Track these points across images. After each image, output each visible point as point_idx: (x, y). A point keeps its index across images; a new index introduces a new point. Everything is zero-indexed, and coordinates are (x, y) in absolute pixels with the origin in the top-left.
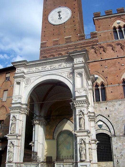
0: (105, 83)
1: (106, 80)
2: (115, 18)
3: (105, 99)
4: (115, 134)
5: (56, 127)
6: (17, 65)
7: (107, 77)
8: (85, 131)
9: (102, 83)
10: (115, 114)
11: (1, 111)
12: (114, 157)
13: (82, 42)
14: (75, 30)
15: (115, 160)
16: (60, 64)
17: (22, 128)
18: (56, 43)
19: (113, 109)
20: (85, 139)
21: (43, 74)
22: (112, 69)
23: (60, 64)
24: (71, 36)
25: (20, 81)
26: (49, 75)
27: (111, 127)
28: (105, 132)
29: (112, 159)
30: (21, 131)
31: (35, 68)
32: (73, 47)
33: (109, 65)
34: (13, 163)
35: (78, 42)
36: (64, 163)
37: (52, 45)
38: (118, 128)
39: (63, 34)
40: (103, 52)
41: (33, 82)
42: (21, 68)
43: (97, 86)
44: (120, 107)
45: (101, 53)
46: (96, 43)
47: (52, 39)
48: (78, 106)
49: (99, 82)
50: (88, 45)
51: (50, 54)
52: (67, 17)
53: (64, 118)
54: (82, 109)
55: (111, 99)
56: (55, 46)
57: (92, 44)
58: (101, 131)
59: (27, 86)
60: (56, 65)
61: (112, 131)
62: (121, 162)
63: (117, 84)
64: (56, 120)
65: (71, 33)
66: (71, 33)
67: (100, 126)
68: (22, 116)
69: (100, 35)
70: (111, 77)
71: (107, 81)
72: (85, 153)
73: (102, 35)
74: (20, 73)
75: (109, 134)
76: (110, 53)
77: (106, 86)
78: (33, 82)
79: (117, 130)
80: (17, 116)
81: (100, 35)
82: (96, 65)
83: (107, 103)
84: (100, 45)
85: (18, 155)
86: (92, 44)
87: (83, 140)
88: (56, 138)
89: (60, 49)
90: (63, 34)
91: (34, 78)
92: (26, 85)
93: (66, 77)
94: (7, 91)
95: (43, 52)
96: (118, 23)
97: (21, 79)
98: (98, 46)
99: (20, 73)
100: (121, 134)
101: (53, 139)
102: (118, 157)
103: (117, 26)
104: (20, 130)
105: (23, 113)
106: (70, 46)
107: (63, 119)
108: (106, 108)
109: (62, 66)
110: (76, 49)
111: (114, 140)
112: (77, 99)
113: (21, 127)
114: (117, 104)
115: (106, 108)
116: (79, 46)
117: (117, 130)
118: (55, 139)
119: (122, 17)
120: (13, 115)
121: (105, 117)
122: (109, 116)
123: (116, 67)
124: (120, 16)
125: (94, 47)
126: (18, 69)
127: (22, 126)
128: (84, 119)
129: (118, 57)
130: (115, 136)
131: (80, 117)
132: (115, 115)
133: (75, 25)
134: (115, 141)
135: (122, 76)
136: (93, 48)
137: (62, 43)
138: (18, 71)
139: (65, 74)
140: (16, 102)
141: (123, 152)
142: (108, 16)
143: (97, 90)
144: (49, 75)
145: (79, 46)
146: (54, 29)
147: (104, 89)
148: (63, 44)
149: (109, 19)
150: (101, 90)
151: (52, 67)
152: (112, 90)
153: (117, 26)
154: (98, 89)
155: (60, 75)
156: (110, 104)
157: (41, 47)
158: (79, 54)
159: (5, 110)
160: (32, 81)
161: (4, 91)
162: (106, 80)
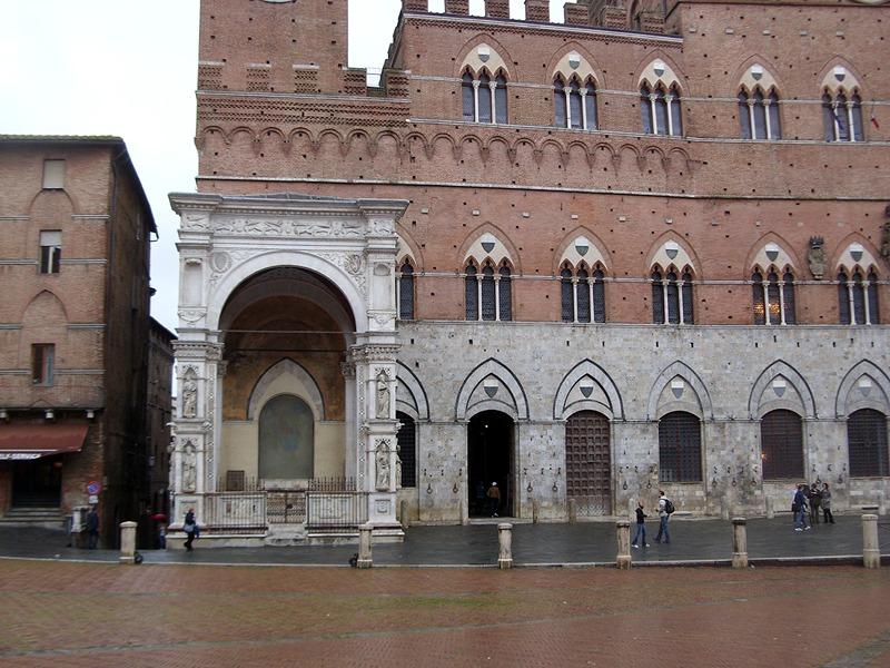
0: (416, 261)
2: (477, 33)
6: (186, 204)
7: (423, 246)
11: (38, 308)
13: (356, 104)
14: (334, 42)
15: (423, 485)
18: (259, 79)
19: (433, 347)
21: (270, 245)
22: (443, 220)
23: (324, 223)
24: (317, 67)
25: (199, 261)
26: (290, 251)
27: (419, 396)
31: (243, 221)
32: (324, 114)
35: (344, 99)
37: (245, 86)
38: (440, 401)
39: (289, 51)
40: (421, 157)
44: (451, 343)
46: (400, 119)
47: (247, 61)
48: (376, 356)
50: (374, 117)
51: (237, 124)
56: (255, 94)
57: (387, 118)
59: (219, 275)
60: (314, 226)
61: (422, 407)
63: (451, 270)
65: (317, 55)
66: (317, 55)
69: (419, 91)
70: (436, 246)
73: (424, 89)
74: (199, 234)
75: (413, 414)
76: (440, 168)
77: (417, 273)
78: (239, 266)
81: (419, 91)
84: (414, 130)
86: (387, 118)
88: (256, 418)
89: (274, 112)
90: (289, 51)
91: (242, 252)
92: (216, 274)
93: (343, 269)
94: (58, 234)
95: (211, 110)
96: (484, 58)
97: (203, 254)
98: (407, 130)
99: (199, 234)
100: (446, 419)
101: (248, 419)
103: (477, 67)
105: (212, 360)
106: (311, 107)
108: (412, 341)
109: (330, 233)
110: (331, 126)
112: (373, 340)
114: (444, 332)
115: (412, 341)
116: (345, 115)
119: (497, 35)
121: (405, 366)
122: (417, 364)
123: (455, 216)
124: (493, 29)
125: (393, 129)
129: (464, 184)
133: (334, 23)
135: (468, 248)
136: (391, 134)
137: (281, 88)
138: (191, 223)
139: (337, 259)
141: (445, 464)
142: (453, 19)
144: (290, 251)
145: (349, 116)
146: (252, 15)
148: (284, 90)
149: (453, 32)
151: (300, 229)
153: (477, 67)
156: (424, 329)
157: (201, 85)
159: (55, 306)
160: (236, 263)
161: (42, 231)
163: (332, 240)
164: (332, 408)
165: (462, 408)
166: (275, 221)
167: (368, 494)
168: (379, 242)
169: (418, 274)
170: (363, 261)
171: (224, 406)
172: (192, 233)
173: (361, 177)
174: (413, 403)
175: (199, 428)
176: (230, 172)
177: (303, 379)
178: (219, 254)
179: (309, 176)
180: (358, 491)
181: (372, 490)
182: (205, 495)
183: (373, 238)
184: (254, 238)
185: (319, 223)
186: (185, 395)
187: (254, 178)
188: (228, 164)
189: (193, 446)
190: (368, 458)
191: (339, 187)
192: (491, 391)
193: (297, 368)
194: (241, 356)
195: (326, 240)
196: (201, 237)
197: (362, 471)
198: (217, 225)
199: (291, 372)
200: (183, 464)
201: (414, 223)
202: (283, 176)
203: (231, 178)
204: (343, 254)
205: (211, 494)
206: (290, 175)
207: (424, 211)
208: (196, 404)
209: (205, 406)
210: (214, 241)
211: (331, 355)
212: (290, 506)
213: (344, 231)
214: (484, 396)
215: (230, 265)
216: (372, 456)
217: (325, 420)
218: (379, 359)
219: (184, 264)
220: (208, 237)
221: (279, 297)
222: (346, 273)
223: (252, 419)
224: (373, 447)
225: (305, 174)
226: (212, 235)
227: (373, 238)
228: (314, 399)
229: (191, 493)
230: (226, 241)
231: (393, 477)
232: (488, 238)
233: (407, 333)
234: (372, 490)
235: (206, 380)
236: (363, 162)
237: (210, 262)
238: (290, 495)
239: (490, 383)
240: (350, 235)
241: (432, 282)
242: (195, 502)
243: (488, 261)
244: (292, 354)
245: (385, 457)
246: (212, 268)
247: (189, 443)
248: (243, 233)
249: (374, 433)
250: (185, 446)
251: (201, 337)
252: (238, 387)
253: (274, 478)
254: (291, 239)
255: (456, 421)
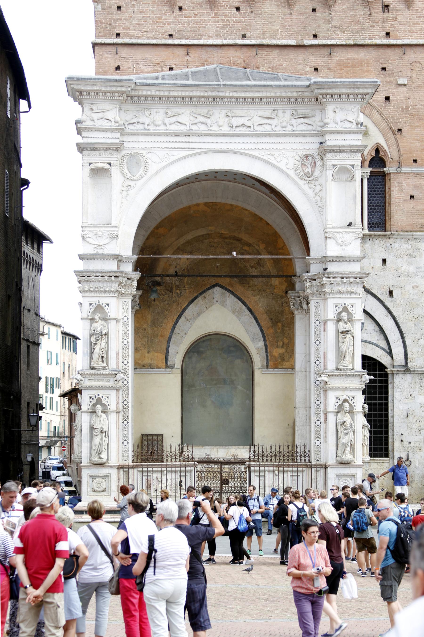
1: (397, 141)
4: (406, 363)
5: (180, 317)
7: (400, 130)
8: (352, 376)
9: (377, 151)
10: (414, 287)
12: (397, 444)
16: (268, 114)
17: (125, 347)
19: (412, 269)
20: (354, 398)
23: (267, 112)
29: (387, 449)
30: (121, 360)
33: (414, 75)
34: (111, 467)
36: (297, 466)
41: (158, 172)
42: (107, 107)
45: (387, 6)
48: (336, 288)
53: (214, 286)
54: (348, 302)
55: (408, 228)
59: (132, 183)
62: (418, 462)
64: (178, 291)
68: (121, 304)
71: (397, 144)
72: (353, 441)
74: (106, 130)
75: (384, 359)
78: (158, 172)
79: (415, 350)
80: (108, 305)
82: (361, 63)
83: (391, 241)
85: (118, 440)
87: (348, 402)
88: (178, 365)
92: (128, 182)
97: (114, 158)
99: (106, 130)
102: (410, 443)
104: (118, 354)
107: (209, 289)
108: (384, 261)
112: (332, 268)
113: (121, 345)
115: (384, 261)
117: (415, 350)
118: (172, 367)
120: (94, 300)
122: (391, 293)
126: (94, 107)
127: (125, 342)
128: (353, 337)
131: (341, 329)
132: (415, 291)
134: (406, 387)
138: (96, 116)
140: (100, 252)
150: (369, 182)
151: (236, 121)
152: (416, 187)
155: (265, 158)
158: (348, 95)
160: (153, 168)
162: (397, 141)
163: (277, 135)
164: (277, 352)
166: (204, 111)
167: (326, 467)
168: (339, 137)
170: (319, 163)
171: (136, 350)
172: (97, 130)
173: (315, 36)
174: (383, 344)
175: (111, 383)
176: (136, 33)
177: (237, 313)
178: (132, 155)
179: (244, 36)
180: (314, 462)
181: (331, 461)
182: (119, 468)
183: (332, 132)
184: (177, 135)
185: (261, 113)
186: (93, 339)
187: (170, 41)
188: (136, 21)
189: (104, 405)
190: (326, 420)
191: (285, 51)
193: (231, 299)
194: (158, 284)
195: (270, 135)
196: (109, 135)
197: (318, 438)
198: (128, 118)
199: (223, 304)
200: (92, 428)
201: (387, 98)
202: (209, 37)
203: (139, 41)
204: (293, 154)
205: (129, 467)
206: (218, 35)
207: (401, 81)
208: (107, 352)
209: (118, 354)
210: (126, 139)
211: (276, 281)
212: (225, 482)
213: (294, 122)
215: (146, 172)
216: (331, 418)
217: (267, 367)
218: (340, 292)
219: (87, 169)
220: (118, 135)
221: (206, 204)
222: (296, 178)
223: (172, 367)
224: (332, 406)
225: (239, 34)
226: (121, 131)
227: (332, 132)
228: (253, 340)
229: (101, 465)
230: (141, 138)
231: (358, 446)
234: (331, 461)
235: (118, 321)
236: (318, 14)
237: (121, 167)
238: (226, 468)
240: (303, 128)
241: (412, 181)
242: (106, 477)
244: (225, 281)
245: (348, 419)
246: (123, 174)
247: (99, 401)
248: (162, 128)
249: (334, 389)
250: (95, 405)
251: (112, 266)
252: (155, 323)
253: (203, 443)
254: (224, 135)
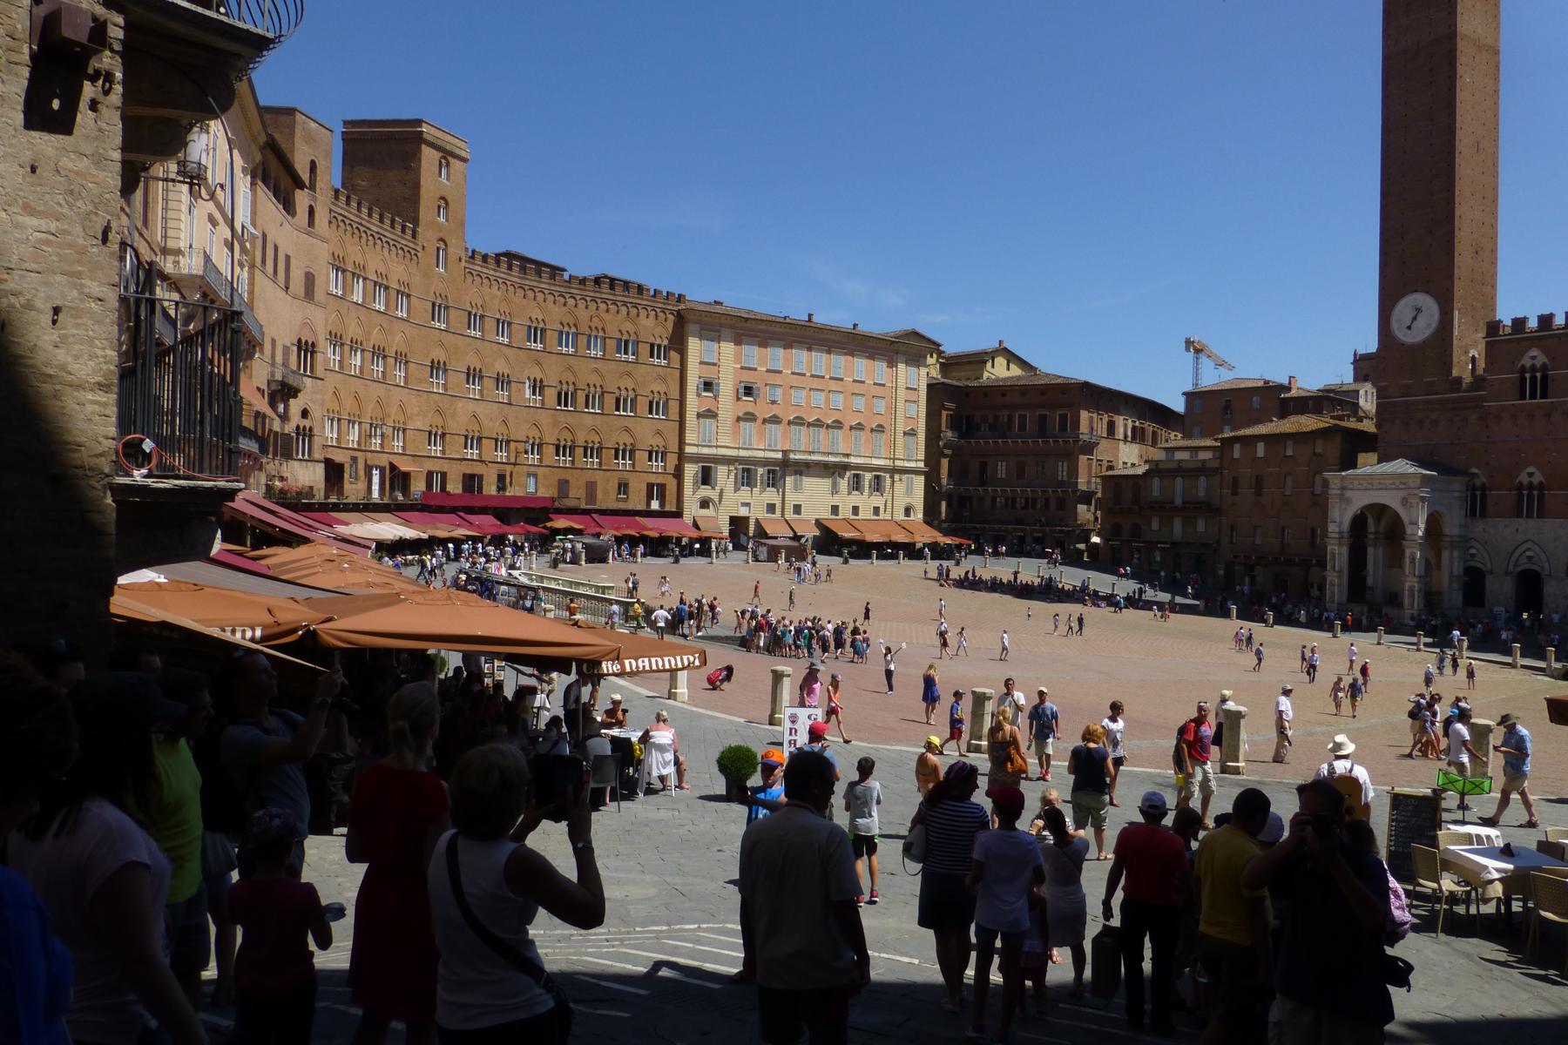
3: (1484, 515)
28: (1479, 565)
43: (1474, 488)
49: (1478, 482)
52: (1429, 325)
58: (1472, 563)
61: (1489, 565)
67: (1473, 555)
75: (1484, 569)
96: (1534, 358)
103: (1527, 362)
111: (1489, 579)
122: (1486, 542)
130: (1491, 572)
135: (1517, 477)
143: (1474, 497)
147: (1484, 496)
154: (1476, 496)
165: (1511, 567)
169: (1488, 492)
192: (1530, 558)
214: (1525, 561)
232: (1531, 469)
233: (1480, 528)
239: (1528, 553)
243: (1531, 483)
251: (1337, 536)
255: (1507, 573)
